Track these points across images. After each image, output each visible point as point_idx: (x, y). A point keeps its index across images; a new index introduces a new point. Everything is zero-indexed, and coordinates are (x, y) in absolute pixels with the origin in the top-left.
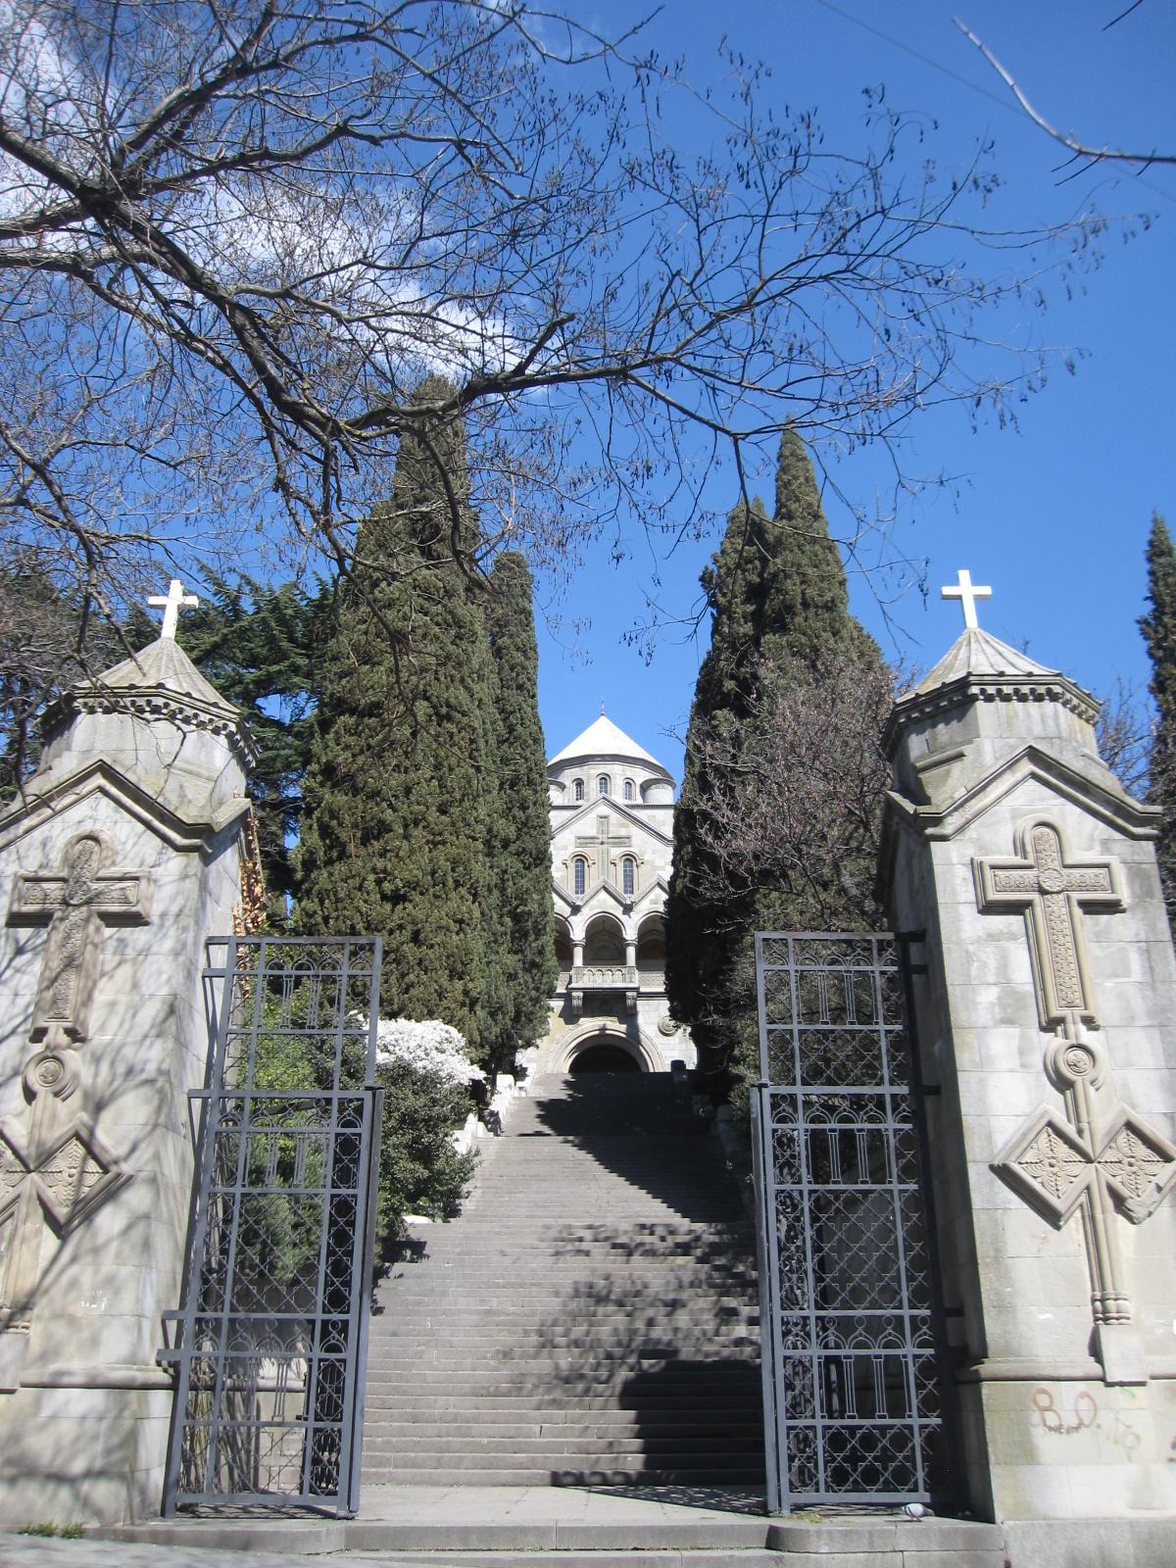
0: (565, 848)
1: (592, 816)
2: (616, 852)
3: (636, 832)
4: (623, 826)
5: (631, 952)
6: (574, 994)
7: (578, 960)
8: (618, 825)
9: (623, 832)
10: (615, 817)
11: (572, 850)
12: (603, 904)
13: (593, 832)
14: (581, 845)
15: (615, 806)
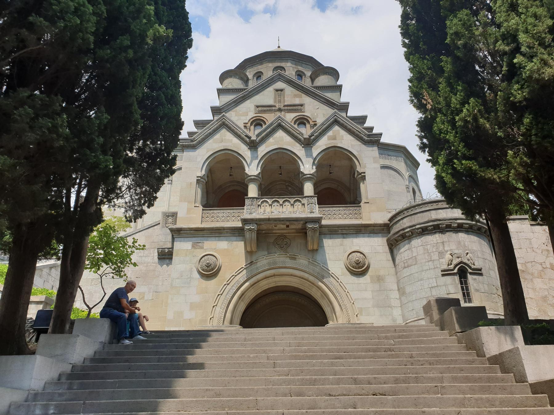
0: (246, 114)
1: (271, 89)
2: (290, 117)
3: (307, 100)
4: (296, 96)
5: (308, 188)
6: (246, 227)
7: (253, 191)
8: (291, 96)
9: (297, 101)
10: (289, 90)
11: (252, 114)
12: (281, 140)
13: (271, 102)
14: (260, 112)
15: (290, 82)
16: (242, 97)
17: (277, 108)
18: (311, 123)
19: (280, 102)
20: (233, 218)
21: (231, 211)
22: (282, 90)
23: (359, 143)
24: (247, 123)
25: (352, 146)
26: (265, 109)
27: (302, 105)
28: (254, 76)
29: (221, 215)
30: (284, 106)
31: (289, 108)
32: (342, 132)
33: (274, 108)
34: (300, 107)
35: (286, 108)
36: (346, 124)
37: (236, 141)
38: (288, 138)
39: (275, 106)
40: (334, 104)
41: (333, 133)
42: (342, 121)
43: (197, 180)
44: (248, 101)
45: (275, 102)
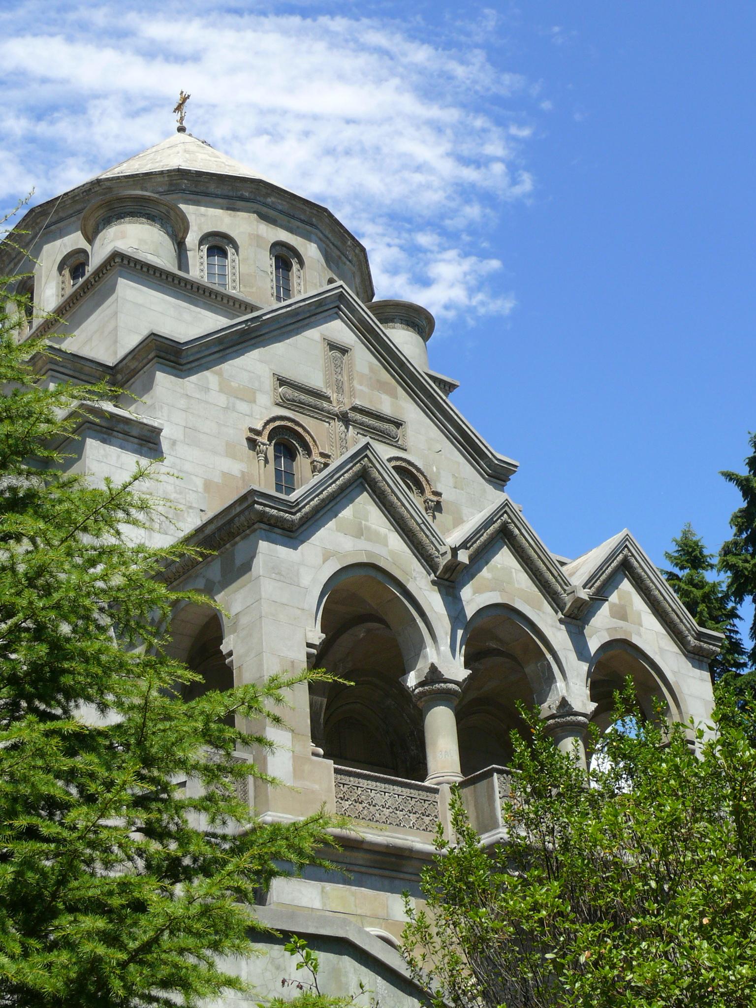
1: (314, 335)
3: (409, 411)
4: (381, 386)
9: (386, 406)
16: (242, 332)
17: (336, 409)
18: (429, 495)
19: (340, 389)
20: (413, 817)
21: (406, 792)
22: (344, 351)
23: (676, 649)
24: (259, 433)
25: (662, 650)
26: (304, 397)
27: (398, 424)
28: (201, 242)
29: (379, 799)
30: (354, 409)
31: (366, 419)
32: (638, 603)
33: (325, 405)
34: (391, 428)
35: (358, 417)
36: (648, 582)
37: (396, 543)
38: (522, 580)
39: (328, 399)
40: (481, 454)
41: (620, 598)
42: (640, 571)
43: (309, 656)
44: (255, 354)
45: (328, 384)
